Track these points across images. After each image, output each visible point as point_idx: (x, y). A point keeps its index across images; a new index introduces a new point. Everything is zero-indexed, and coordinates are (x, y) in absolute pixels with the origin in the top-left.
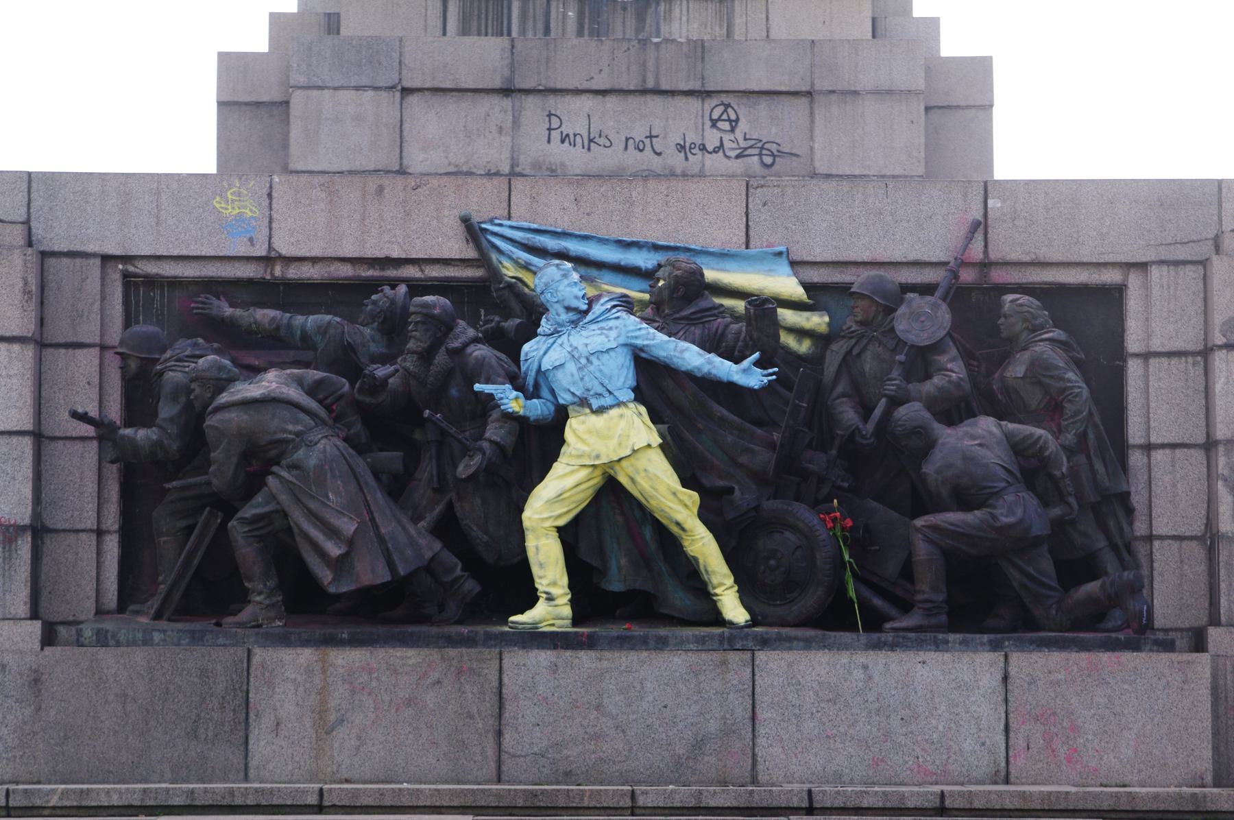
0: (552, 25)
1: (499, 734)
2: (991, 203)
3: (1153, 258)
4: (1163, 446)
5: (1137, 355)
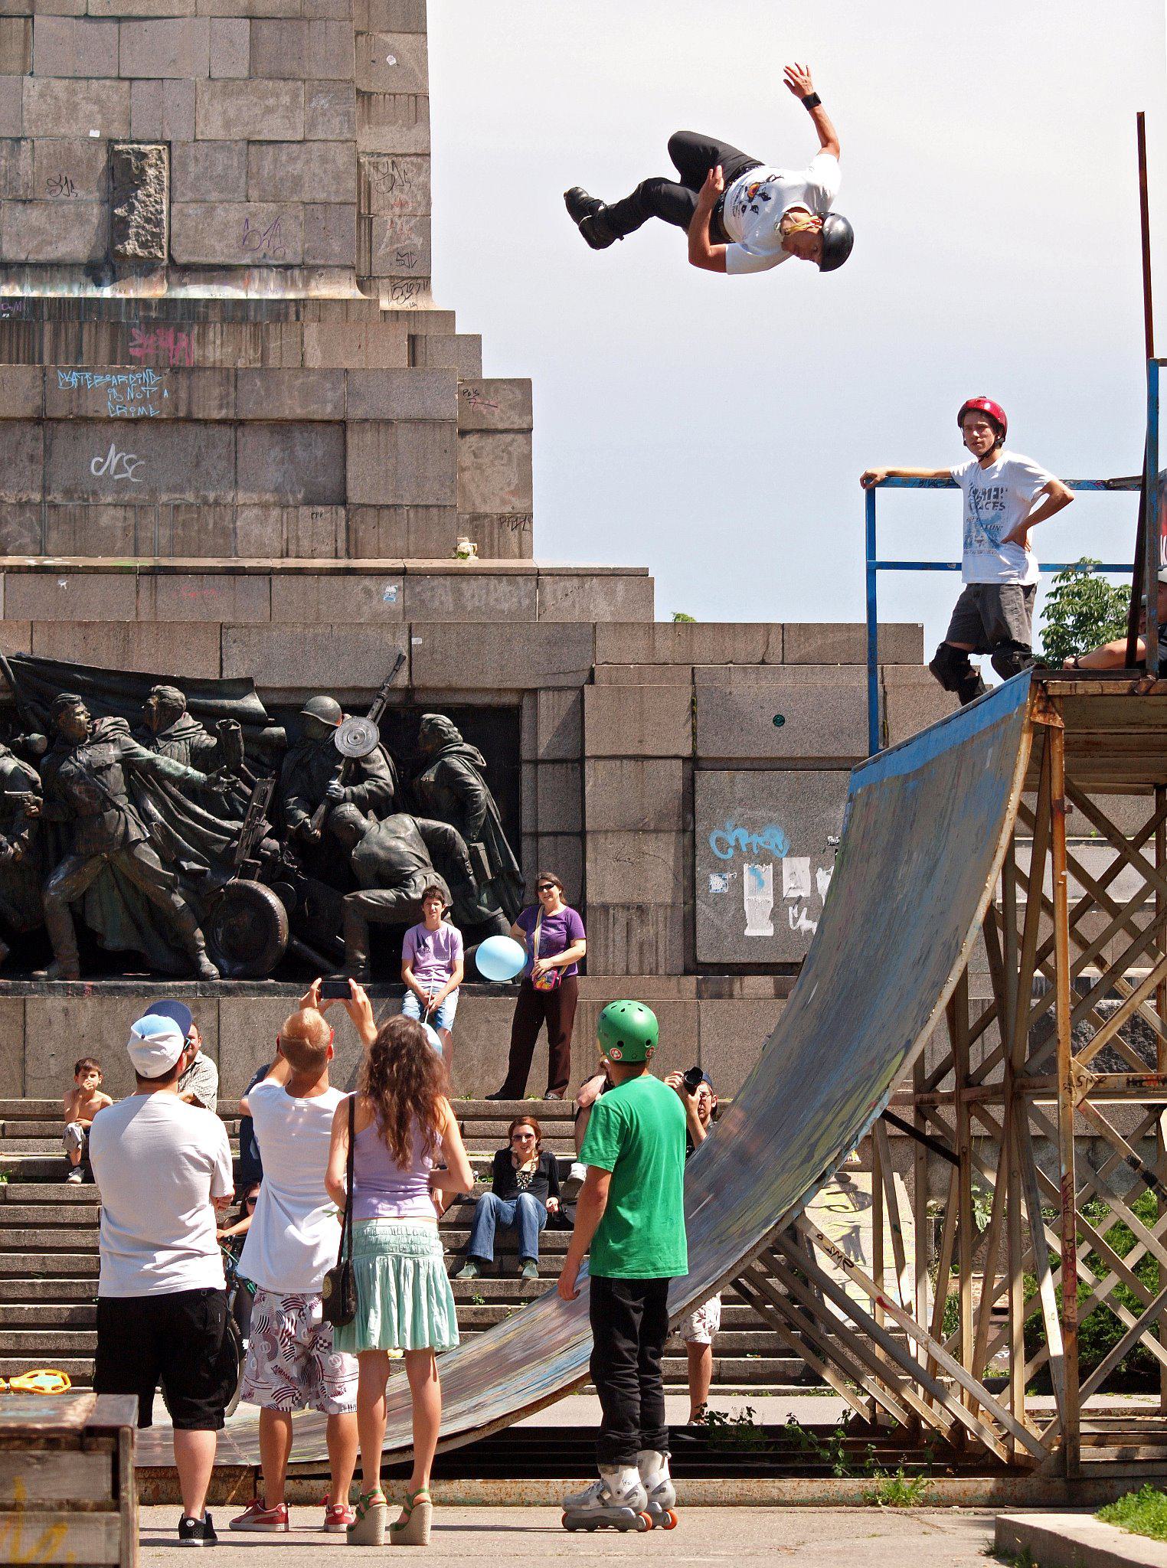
0: (85, 348)
1: (24, 1061)
2: (414, 641)
3: (542, 685)
4: (548, 834)
5: (529, 762)
